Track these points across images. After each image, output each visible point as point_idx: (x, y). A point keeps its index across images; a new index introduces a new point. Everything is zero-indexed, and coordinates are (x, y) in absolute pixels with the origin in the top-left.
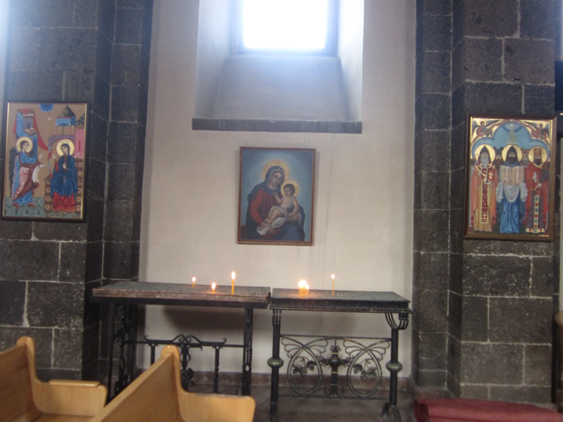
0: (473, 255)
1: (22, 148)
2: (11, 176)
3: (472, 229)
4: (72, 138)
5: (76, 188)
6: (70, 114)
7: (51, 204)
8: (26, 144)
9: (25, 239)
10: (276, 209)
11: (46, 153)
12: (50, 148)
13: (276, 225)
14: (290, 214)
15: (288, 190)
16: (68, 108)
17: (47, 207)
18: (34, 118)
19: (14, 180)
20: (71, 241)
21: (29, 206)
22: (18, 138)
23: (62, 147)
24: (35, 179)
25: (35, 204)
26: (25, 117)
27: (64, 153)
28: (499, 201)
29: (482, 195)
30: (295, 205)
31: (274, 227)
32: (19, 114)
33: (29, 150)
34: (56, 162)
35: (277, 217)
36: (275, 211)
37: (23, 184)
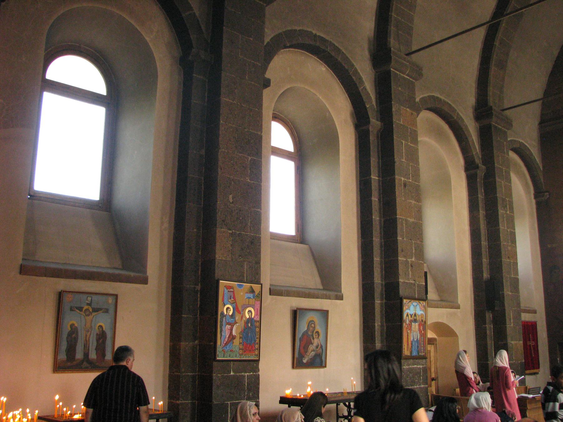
0: (404, 367)
1: (227, 312)
2: (221, 331)
3: (404, 354)
4: (253, 306)
5: (255, 339)
6: (252, 291)
7: (242, 350)
8: (229, 309)
9: (228, 374)
10: (311, 346)
11: (240, 315)
12: (242, 313)
13: (311, 356)
14: (317, 349)
15: (317, 335)
16: (251, 287)
17: (241, 351)
18: (233, 292)
19: (223, 334)
20: (252, 373)
21: (231, 351)
22: (225, 305)
23: (248, 312)
24: (234, 333)
25: (234, 350)
26: (229, 291)
27: (249, 316)
28: (412, 340)
29: (407, 337)
30: (319, 344)
31: (310, 358)
32: (225, 290)
33: (231, 313)
34: (245, 322)
35: (312, 351)
36: (311, 347)
37: (227, 337)
